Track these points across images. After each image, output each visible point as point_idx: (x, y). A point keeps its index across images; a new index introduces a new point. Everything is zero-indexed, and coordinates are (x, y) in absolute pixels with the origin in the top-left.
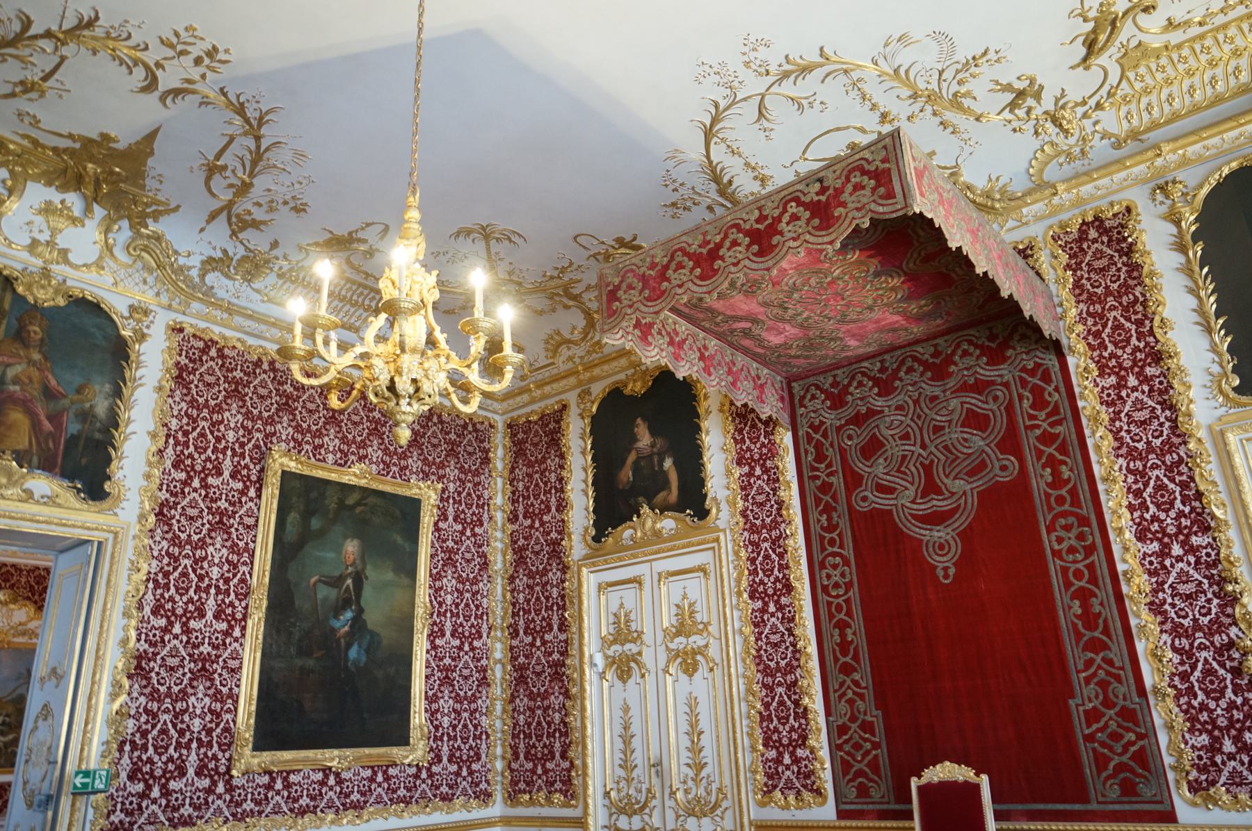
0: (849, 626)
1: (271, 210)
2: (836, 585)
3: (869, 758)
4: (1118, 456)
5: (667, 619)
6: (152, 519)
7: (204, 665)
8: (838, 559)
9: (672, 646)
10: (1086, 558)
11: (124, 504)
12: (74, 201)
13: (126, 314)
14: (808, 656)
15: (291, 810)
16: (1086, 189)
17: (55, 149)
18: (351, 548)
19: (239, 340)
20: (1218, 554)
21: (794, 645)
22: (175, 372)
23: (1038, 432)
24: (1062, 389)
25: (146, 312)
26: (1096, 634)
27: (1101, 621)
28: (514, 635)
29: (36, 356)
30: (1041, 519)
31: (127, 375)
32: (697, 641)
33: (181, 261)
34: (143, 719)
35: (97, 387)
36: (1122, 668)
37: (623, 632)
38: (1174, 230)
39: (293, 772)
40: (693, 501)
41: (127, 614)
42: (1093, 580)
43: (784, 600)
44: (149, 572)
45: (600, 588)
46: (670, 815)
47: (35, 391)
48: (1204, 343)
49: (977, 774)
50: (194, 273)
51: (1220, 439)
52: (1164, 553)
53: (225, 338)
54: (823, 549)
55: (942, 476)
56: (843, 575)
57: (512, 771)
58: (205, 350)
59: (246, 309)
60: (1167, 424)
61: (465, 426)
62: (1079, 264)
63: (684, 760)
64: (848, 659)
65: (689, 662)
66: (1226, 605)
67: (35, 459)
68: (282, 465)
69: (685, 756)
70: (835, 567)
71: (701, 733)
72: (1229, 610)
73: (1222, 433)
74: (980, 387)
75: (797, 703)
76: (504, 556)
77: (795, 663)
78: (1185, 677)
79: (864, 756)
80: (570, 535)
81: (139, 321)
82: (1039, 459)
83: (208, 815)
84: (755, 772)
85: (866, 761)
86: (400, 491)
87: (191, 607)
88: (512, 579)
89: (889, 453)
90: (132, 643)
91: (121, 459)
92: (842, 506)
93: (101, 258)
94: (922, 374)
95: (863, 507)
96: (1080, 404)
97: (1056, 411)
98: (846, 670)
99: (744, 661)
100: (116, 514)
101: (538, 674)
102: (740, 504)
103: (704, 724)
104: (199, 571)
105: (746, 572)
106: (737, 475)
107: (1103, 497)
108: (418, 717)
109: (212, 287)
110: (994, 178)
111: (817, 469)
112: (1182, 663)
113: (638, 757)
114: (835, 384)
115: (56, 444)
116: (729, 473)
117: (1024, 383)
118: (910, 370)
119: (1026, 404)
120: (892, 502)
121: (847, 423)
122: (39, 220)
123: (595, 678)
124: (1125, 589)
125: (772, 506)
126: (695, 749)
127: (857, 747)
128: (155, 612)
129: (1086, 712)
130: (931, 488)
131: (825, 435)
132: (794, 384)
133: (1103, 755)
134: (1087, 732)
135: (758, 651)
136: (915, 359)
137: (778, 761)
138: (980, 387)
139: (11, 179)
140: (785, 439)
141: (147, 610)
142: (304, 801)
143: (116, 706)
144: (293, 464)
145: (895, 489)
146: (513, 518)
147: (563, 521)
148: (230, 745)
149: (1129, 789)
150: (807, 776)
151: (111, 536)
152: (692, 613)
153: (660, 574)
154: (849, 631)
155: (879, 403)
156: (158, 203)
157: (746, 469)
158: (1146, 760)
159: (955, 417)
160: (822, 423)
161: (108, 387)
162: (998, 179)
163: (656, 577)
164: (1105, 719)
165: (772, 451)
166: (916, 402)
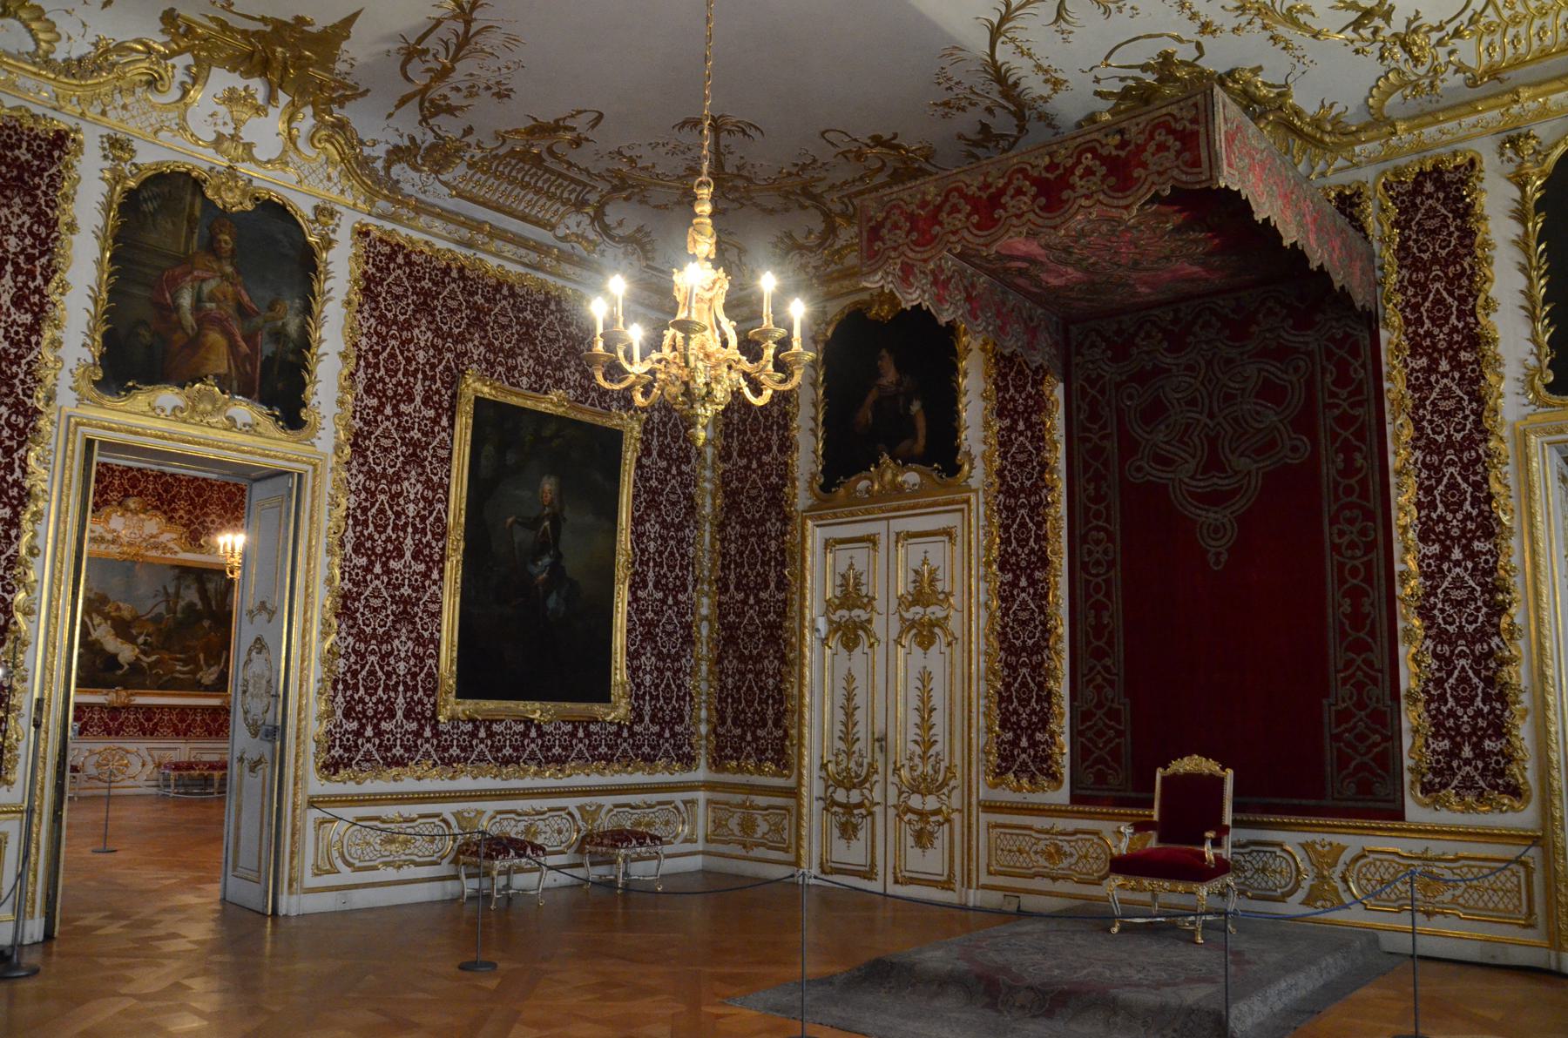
1: (471, 95)
2: (1098, 563)
4: (1415, 448)
5: (902, 586)
6: (348, 450)
9: (908, 615)
10: (1365, 554)
11: (321, 433)
12: (258, 86)
13: (312, 217)
14: (1060, 637)
15: (496, 759)
16: (1430, 132)
17: (244, 33)
18: (548, 485)
19: (426, 243)
20: (1496, 562)
21: (1044, 624)
22: (362, 284)
23: (1337, 412)
24: (1370, 367)
25: (332, 214)
26: (1362, 635)
28: (724, 589)
29: (229, 269)
31: (316, 288)
32: (936, 612)
33: (367, 151)
34: (352, 659)
35: (288, 303)
36: (1381, 671)
37: (851, 595)
38: (1517, 194)
40: (942, 454)
41: (330, 552)
42: (1368, 579)
43: (1037, 575)
45: (829, 544)
46: (892, 792)
48: (1525, 330)
50: (379, 165)
51: (1522, 440)
52: (1444, 556)
53: (411, 241)
54: (1087, 522)
55: (1227, 451)
56: (1105, 552)
57: (718, 736)
58: (391, 258)
59: (434, 206)
60: (1472, 417)
62: (1408, 221)
63: (911, 736)
64: (1101, 644)
65: (925, 634)
66: (1493, 615)
67: (235, 384)
68: (475, 390)
69: (913, 733)
70: (1098, 542)
71: (932, 710)
72: (1495, 620)
73: (1525, 435)
75: (1041, 686)
76: (714, 499)
77: (1043, 644)
78: (1439, 683)
79: (1106, 744)
80: (793, 483)
81: (325, 225)
84: (988, 753)
86: (599, 421)
88: (722, 527)
91: (315, 383)
93: (284, 151)
96: (1386, 385)
97: (1359, 391)
98: (1099, 654)
99: (987, 637)
100: (313, 444)
101: (751, 636)
103: (937, 700)
106: (996, 428)
107: (1393, 491)
108: (620, 674)
109: (398, 181)
110: (1327, 104)
111: (1090, 430)
112: (1439, 669)
113: (861, 731)
116: (987, 425)
117: (1330, 354)
119: (1329, 379)
122: (223, 110)
123: (817, 644)
124: (1398, 591)
126: (925, 724)
127: (1100, 734)
128: (356, 550)
129: (1337, 712)
130: (1213, 464)
131: (1102, 392)
132: (1072, 327)
134: (1335, 731)
135: (1003, 628)
137: (1015, 743)
139: (197, 65)
140: (1057, 392)
141: (349, 547)
142: (557, 750)
143: (327, 645)
144: (486, 389)
145: (1174, 461)
146: (725, 456)
147: (786, 464)
148: (434, 690)
149: (1365, 788)
151: (310, 468)
152: (932, 581)
153: (898, 534)
156: (346, 87)
157: (1008, 422)
158: (1388, 761)
160: (1100, 377)
161: (297, 303)
162: (1331, 106)
163: (893, 538)
165: (1040, 404)
166: (1209, 363)
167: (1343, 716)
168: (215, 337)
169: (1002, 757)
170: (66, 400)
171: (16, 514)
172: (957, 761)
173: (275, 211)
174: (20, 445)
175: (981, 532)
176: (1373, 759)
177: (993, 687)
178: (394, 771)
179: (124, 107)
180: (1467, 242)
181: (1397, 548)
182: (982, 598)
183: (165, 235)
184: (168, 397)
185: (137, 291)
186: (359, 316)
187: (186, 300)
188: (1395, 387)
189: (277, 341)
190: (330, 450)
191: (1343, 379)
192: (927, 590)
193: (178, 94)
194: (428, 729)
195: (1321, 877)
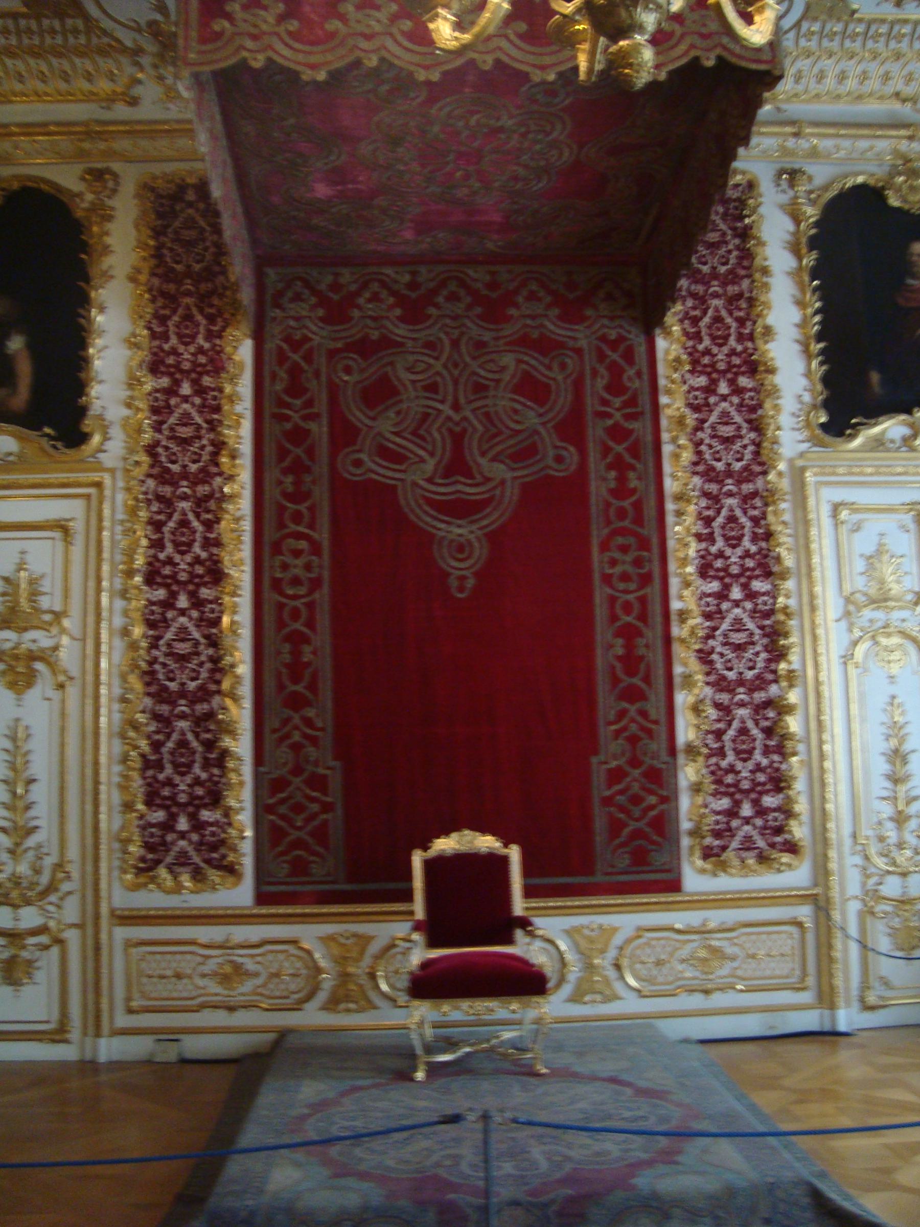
0: (307, 641)
3: (316, 823)
8: (303, 544)
10: (641, 588)
14: (238, 679)
20: (774, 604)
21: (215, 660)
23: (610, 422)
24: (645, 377)
27: (642, 666)
30: (595, 533)
32: (39, 639)
38: (791, 227)
42: (643, 617)
43: (205, 593)
48: (799, 366)
49: (506, 846)
51: (798, 474)
54: (281, 525)
56: (308, 567)
64: (299, 688)
70: (297, 553)
71: (31, 781)
73: (803, 470)
74: (545, 346)
75: (209, 745)
78: (719, 735)
82: (605, 456)
85: (309, 828)
89: (404, 406)
92: (322, 468)
94: (469, 307)
95: (353, 474)
96: (664, 400)
97: (633, 402)
98: (296, 702)
99: (124, 677)
102: (148, 436)
105: (144, 542)
106: (148, 387)
107: (670, 519)
111: (288, 406)
114: (335, 287)
116: (133, 382)
117: (601, 357)
118: (453, 297)
119: (601, 383)
120: (397, 475)
121: (349, 348)
124: (675, 631)
125: (203, 448)
127: (298, 808)
130: (457, 466)
133: (619, 820)
135: (151, 663)
136: (462, 284)
137: (168, 826)
138: (545, 346)
149: (640, 859)
150: (214, 847)
152: (34, 594)
154: (307, 649)
155: (401, 331)
157: (165, 382)
158: (663, 826)
159: (506, 377)
160: (306, 339)
164: (628, 779)
165: (217, 364)
166: (455, 343)
167: (616, 776)
169: (149, 847)
172: (73, 852)
175: (119, 528)
176: (650, 824)
177: (136, 747)
180: (745, 263)
181: (674, 583)
182: (118, 621)
188: (673, 405)
191: (616, 387)
192: (24, 604)
195: (590, 967)
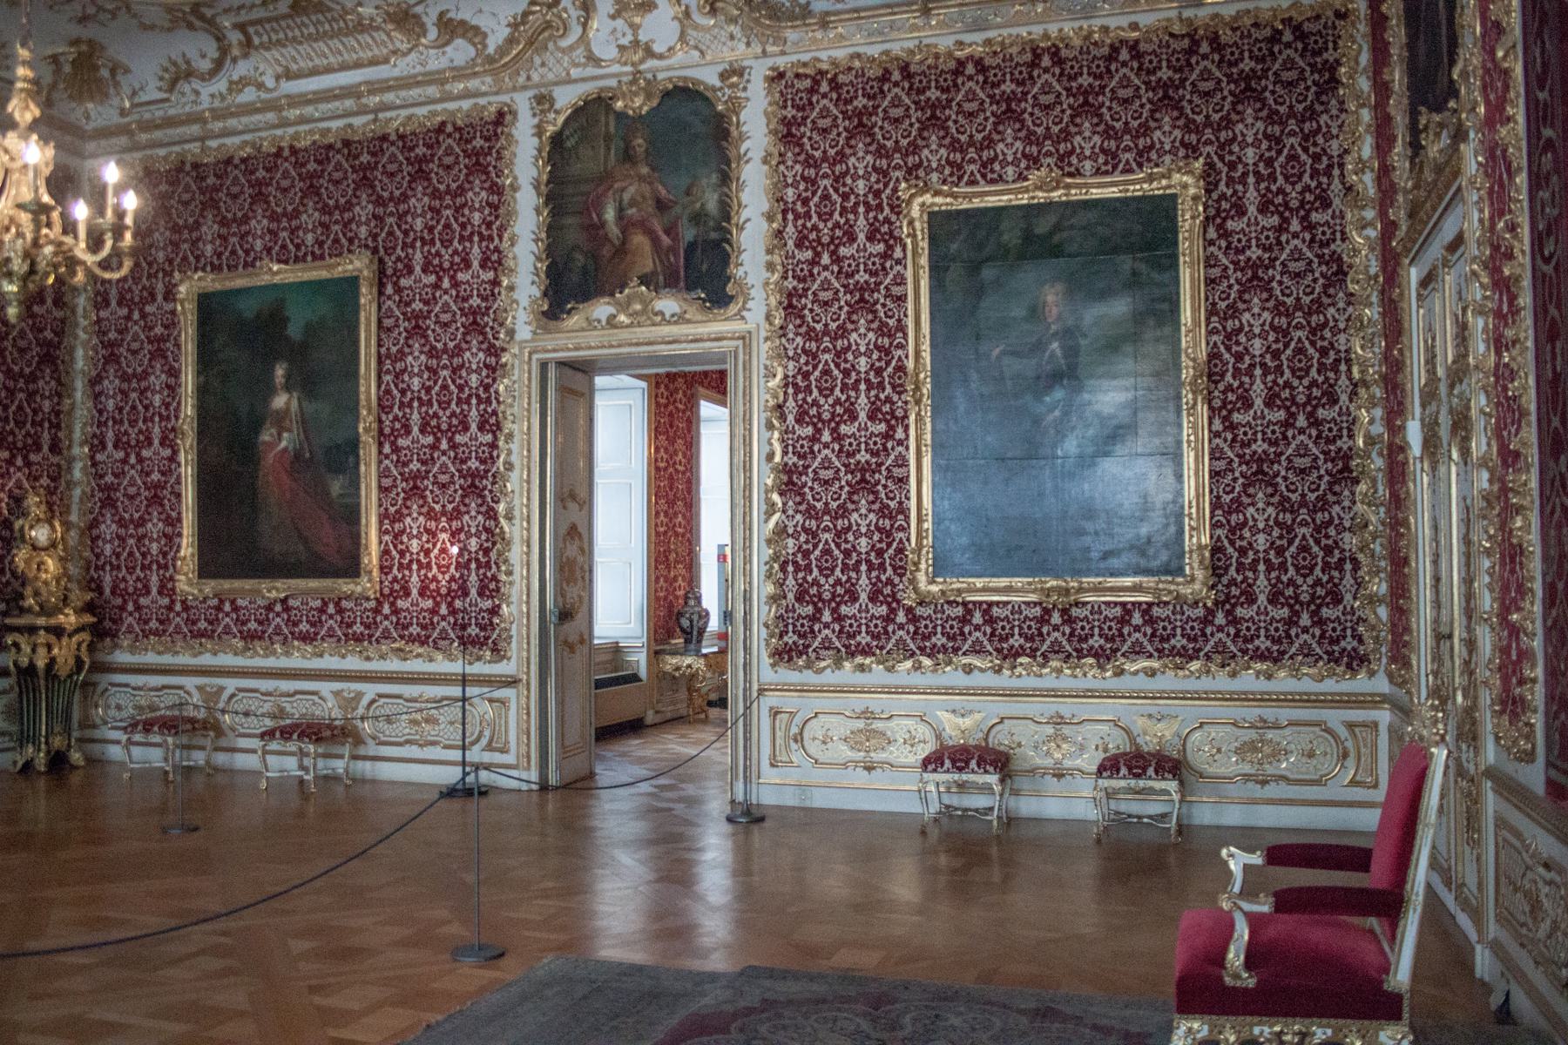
7: (863, 476)
11: (750, 304)
13: (718, 84)
29: (645, 170)
31: (732, 154)
39: (998, 603)
44: (786, 377)
47: (650, 207)
53: (834, 63)
61: (1276, 37)
67: (661, 278)
83: (890, 646)
87: (839, 410)
90: (777, 459)
91: (740, 253)
93: (683, 33)
100: (743, 318)
104: (843, 365)
115: (676, 255)
122: (619, 23)
141: (791, 418)
161: (714, 178)
168: (639, 240)
170: (524, 333)
171: (496, 438)
173: (685, 94)
174: (494, 380)
178: (859, 659)
179: (543, 65)
183: (587, 162)
184: (602, 309)
185: (569, 220)
186: (782, 168)
187: (610, 214)
189: (697, 224)
190: (761, 319)
193: (579, 30)
194: (331, 606)
